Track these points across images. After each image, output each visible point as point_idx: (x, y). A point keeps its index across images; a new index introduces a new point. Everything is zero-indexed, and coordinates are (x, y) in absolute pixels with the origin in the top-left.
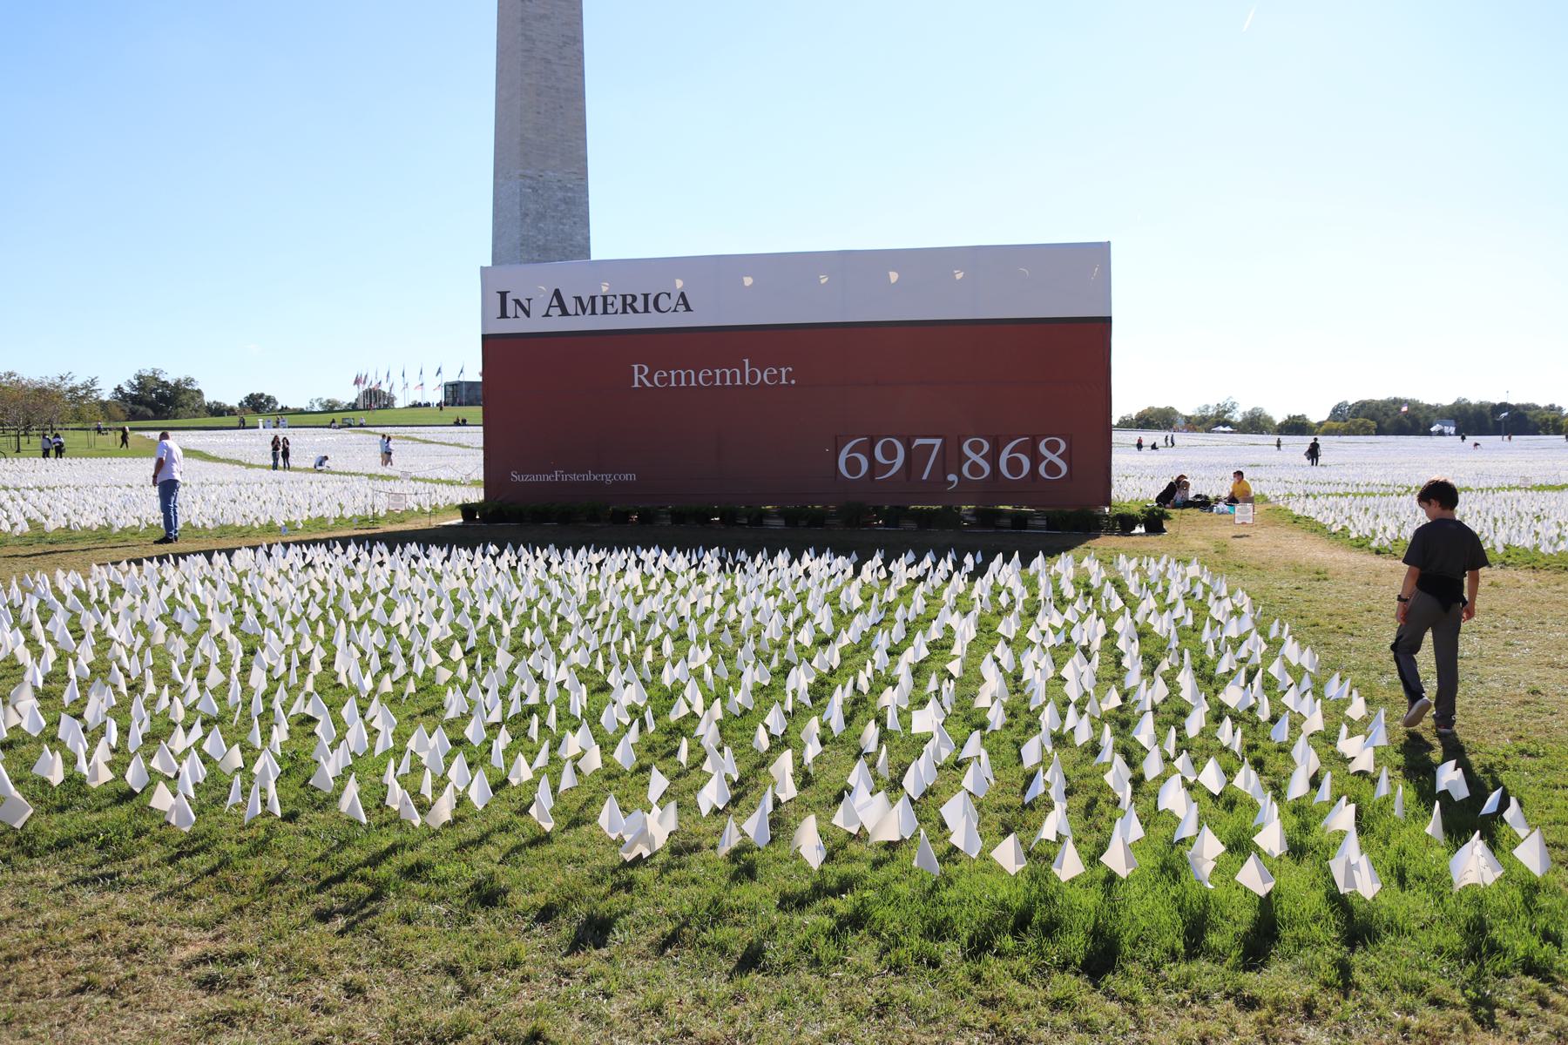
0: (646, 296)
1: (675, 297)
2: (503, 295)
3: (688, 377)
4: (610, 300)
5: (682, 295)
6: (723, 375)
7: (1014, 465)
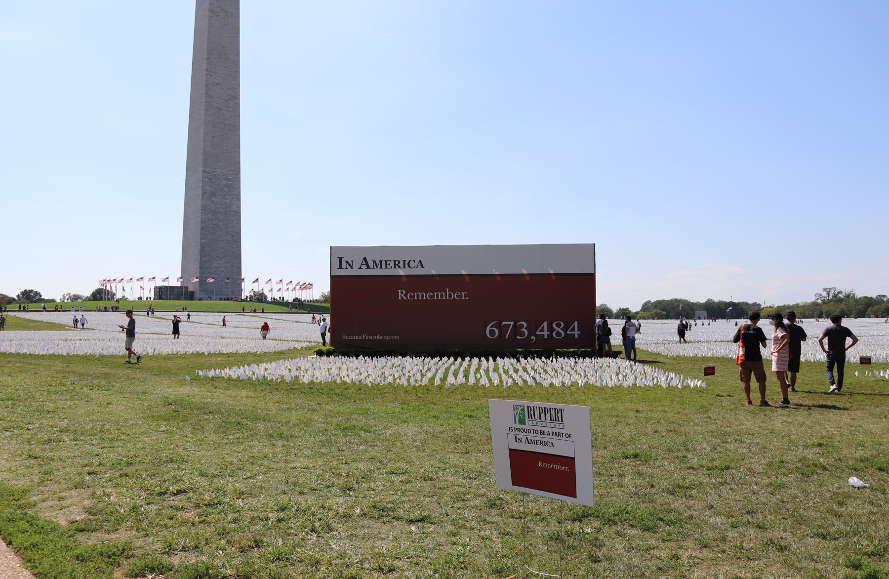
1: (417, 262)
2: (341, 259)
6: (437, 295)
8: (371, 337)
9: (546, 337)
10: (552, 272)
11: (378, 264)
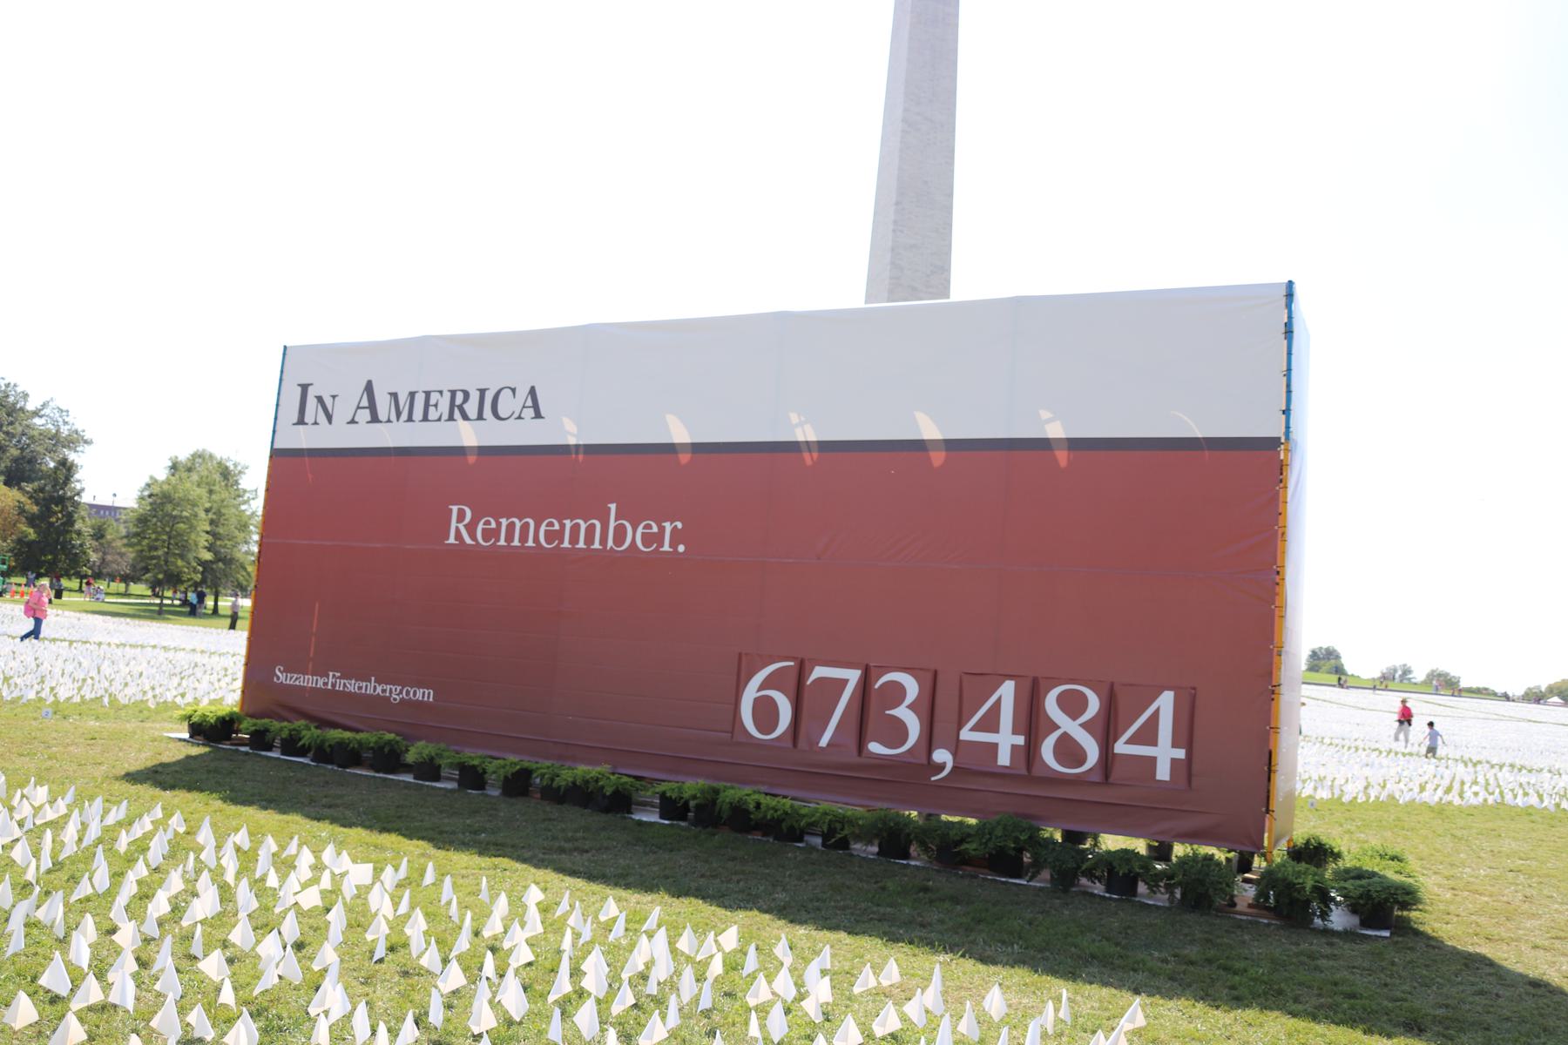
0: (482, 392)
1: (523, 392)
2: (304, 388)
4: (434, 398)
5: (533, 392)
9: (1004, 759)
10: (1055, 431)
11: (403, 408)
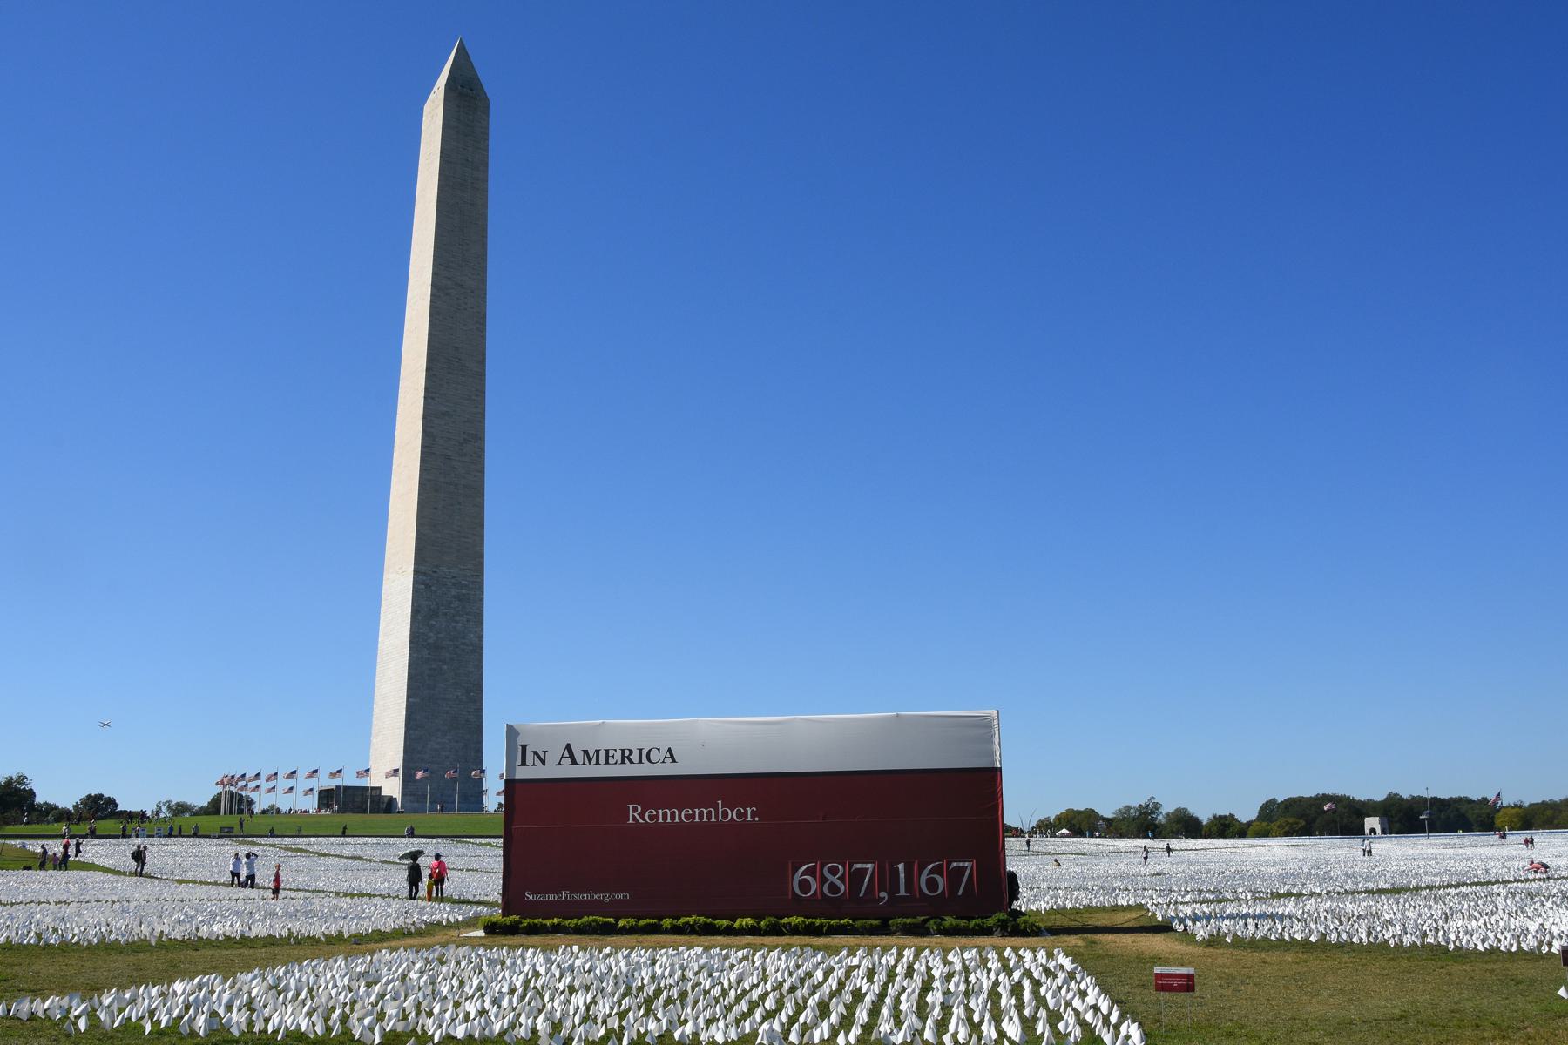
1: (664, 751)
3: (673, 815)
6: (701, 814)
7: (932, 884)
8: (578, 897)
11: (592, 757)
